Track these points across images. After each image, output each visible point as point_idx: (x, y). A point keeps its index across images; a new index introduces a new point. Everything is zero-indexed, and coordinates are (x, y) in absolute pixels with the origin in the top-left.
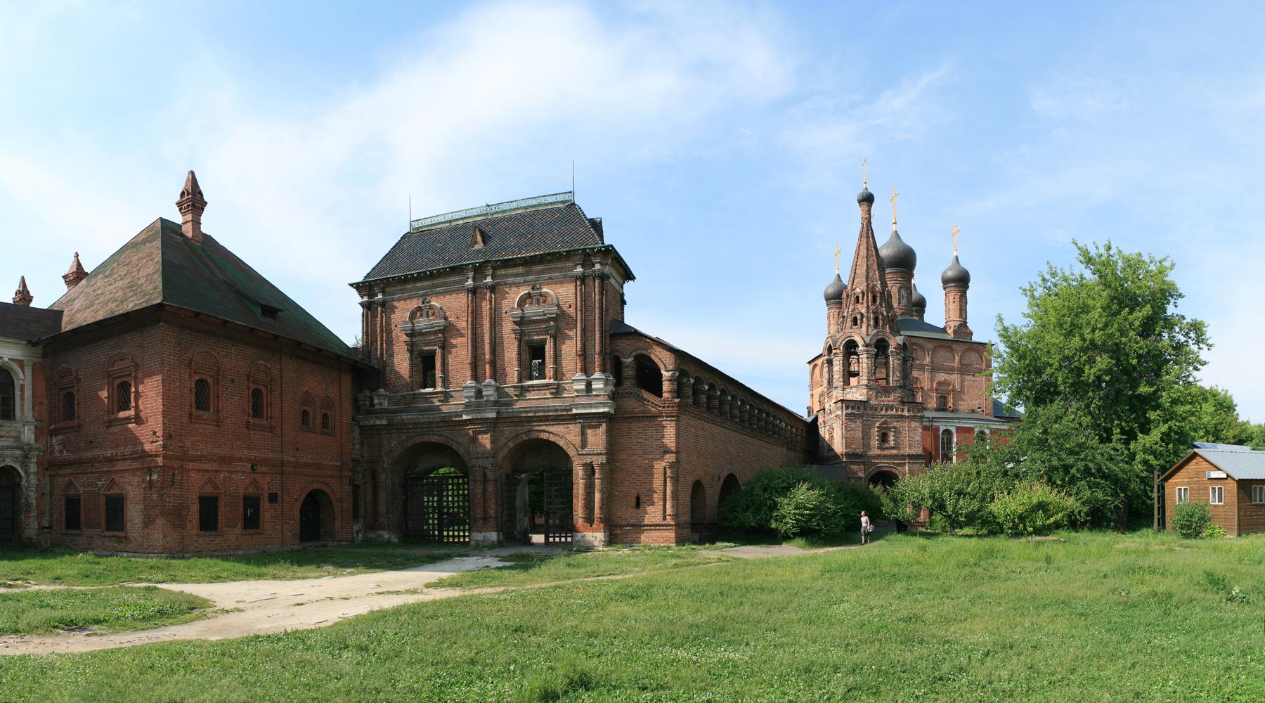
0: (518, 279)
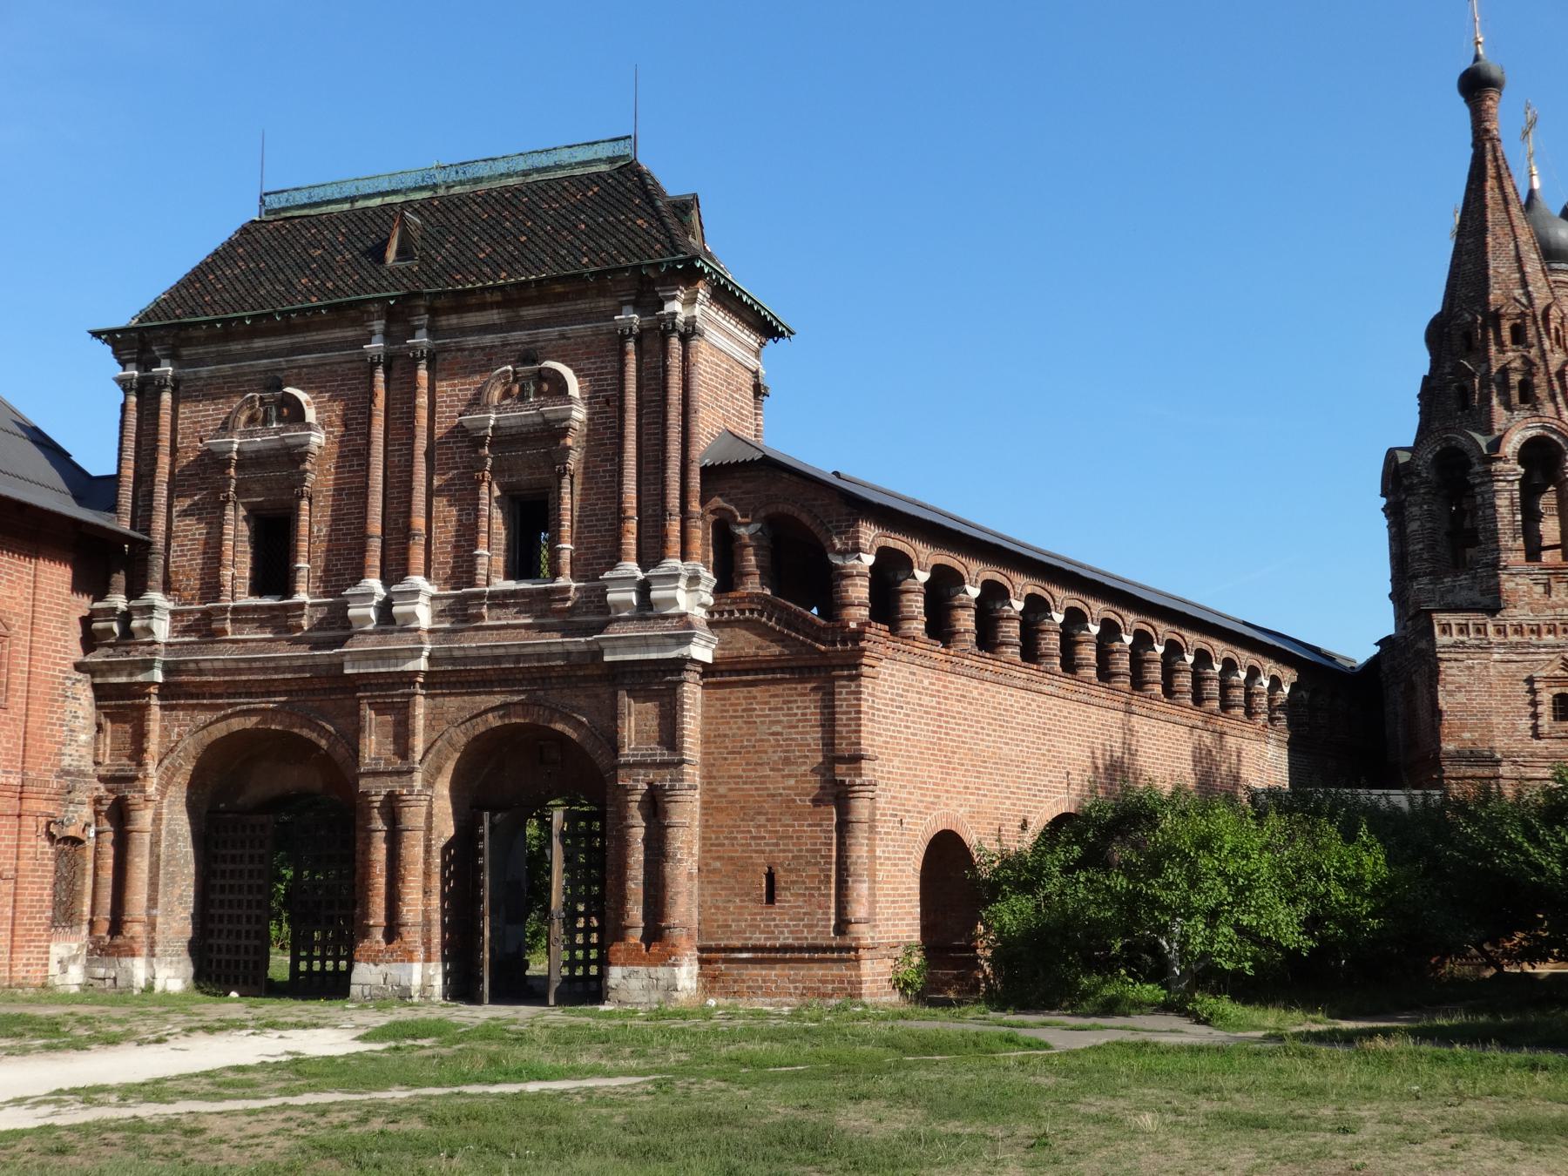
0: (489, 339)
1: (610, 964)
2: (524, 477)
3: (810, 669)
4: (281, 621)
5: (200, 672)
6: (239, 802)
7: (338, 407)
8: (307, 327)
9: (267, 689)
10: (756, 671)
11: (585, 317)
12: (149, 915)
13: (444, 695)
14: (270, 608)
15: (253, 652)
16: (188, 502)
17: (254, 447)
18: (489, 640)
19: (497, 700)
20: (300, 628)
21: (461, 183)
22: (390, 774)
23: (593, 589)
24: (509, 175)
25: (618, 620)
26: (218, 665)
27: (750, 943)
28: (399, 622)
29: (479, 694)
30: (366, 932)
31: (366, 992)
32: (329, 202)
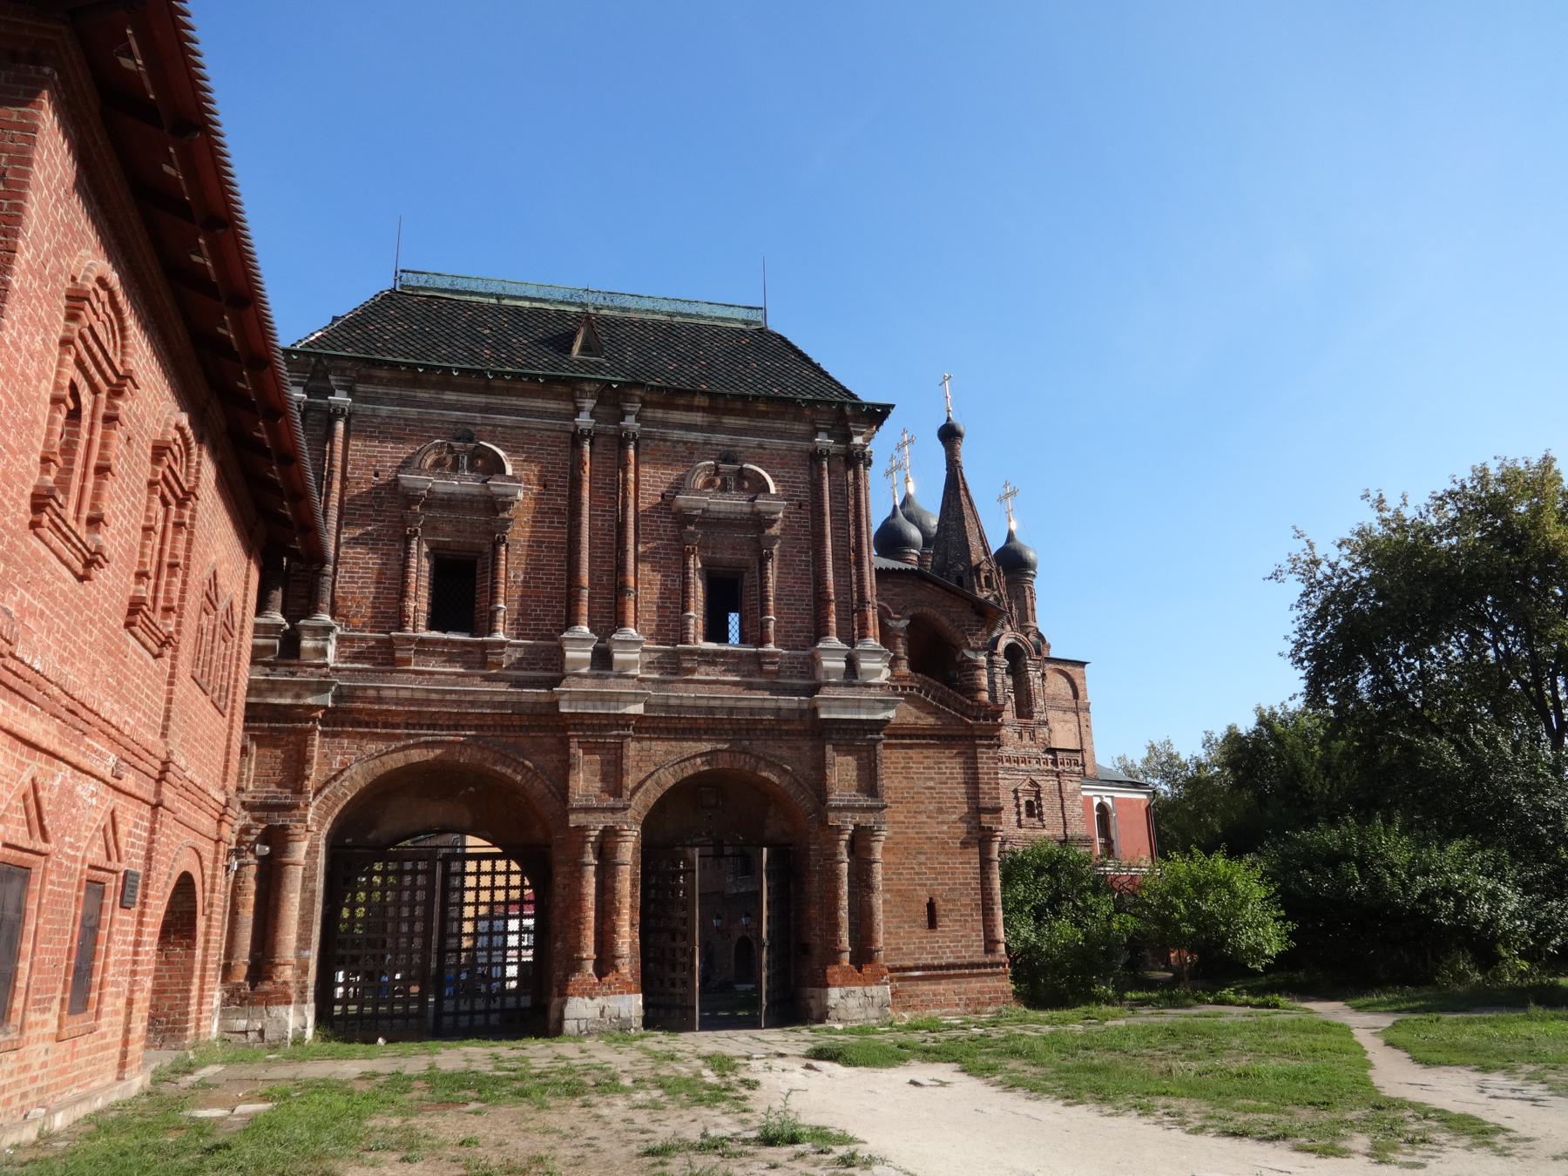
0: (693, 436)
1: (828, 986)
2: (726, 556)
3: (953, 737)
4: (479, 658)
5: (380, 700)
6: (370, 837)
7: (535, 469)
8: (508, 392)
9: (456, 723)
11: (781, 435)
12: (298, 957)
13: (650, 739)
14: (464, 643)
15: (445, 683)
16: (358, 532)
17: (449, 489)
18: (704, 692)
19: (706, 747)
21: (608, 308)
22: (603, 810)
24: (654, 312)
25: (828, 684)
26: (403, 694)
27: (921, 963)
29: (687, 740)
30: (576, 965)
31: (583, 1027)
32: (472, 293)
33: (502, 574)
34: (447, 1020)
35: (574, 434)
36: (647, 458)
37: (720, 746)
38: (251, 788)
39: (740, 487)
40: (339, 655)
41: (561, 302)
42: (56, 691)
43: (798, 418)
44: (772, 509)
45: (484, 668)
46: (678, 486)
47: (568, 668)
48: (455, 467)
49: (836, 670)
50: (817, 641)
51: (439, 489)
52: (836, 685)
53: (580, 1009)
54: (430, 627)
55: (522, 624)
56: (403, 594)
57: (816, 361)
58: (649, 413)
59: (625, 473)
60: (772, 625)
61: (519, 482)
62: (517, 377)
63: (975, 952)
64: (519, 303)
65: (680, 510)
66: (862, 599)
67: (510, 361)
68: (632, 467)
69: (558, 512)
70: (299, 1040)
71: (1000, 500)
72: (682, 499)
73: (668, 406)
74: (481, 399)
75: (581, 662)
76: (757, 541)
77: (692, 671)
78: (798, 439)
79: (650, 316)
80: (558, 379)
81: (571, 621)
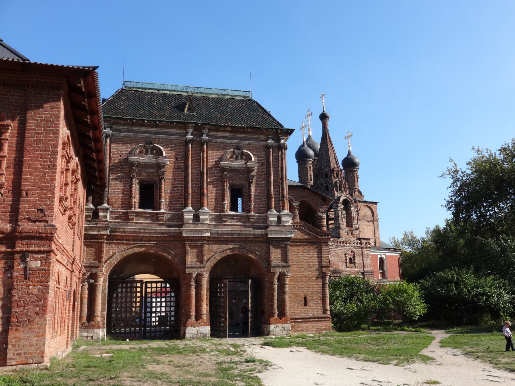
0: (226, 141)
1: (270, 324)
2: (237, 182)
3: (314, 242)
4: (156, 218)
5: (124, 232)
6: (121, 276)
7: (173, 153)
8: (163, 127)
9: (149, 239)
10: (299, 242)
11: (256, 140)
12: (102, 314)
13: (212, 244)
14: (151, 213)
15: (145, 226)
16: (115, 176)
17: (145, 161)
18: (230, 229)
19: (231, 246)
20: (162, 220)
21: (196, 93)
22: (197, 268)
23: (178, 215)
24: (212, 94)
25: (271, 226)
26: (132, 230)
27: (301, 317)
28: (201, 221)
29: (224, 244)
30: (189, 317)
31: (191, 336)
32: (149, 89)
33: (163, 189)
34: (148, 334)
35: (186, 141)
36: (210, 149)
37: (235, 246)
38: (85, 261)
39: (242, 158)
40: (111, 217)
41: (180, 91)
42: (62, 247)
43: (262, 134)
44: (253, 166)
45: (157, 221)
46: (221, 159)
47: (185, 221)
48: (146, 153)
49: (274, 221)
50: (268, 211)
51: (141, 161)
52: (274, 226)
53: (190, 331)
54: (140, 208)
55: (171, 206)
56: (131, 197)
57: (267, 109)
58: (211, 133)
59: (203, 154)
60: (253, 206)
61: (168, 158)
62: (167, 122)
63: (320, 313)
64: (166, 92)
65: (222, 167)
66: (283, 197)
67: (164, 115)
68: (205, 152)
69: (181, 168)
70: (103, 340)
71: (346, 138)
72: (222, 163)
73: (217, 130)
74: (154, 130)
75: (189, 219)
76: (248, 177)
77: (226, 221)
78: (262, 141)
79: (211, 96)
80: (180, 123)
81: (186, 205)
